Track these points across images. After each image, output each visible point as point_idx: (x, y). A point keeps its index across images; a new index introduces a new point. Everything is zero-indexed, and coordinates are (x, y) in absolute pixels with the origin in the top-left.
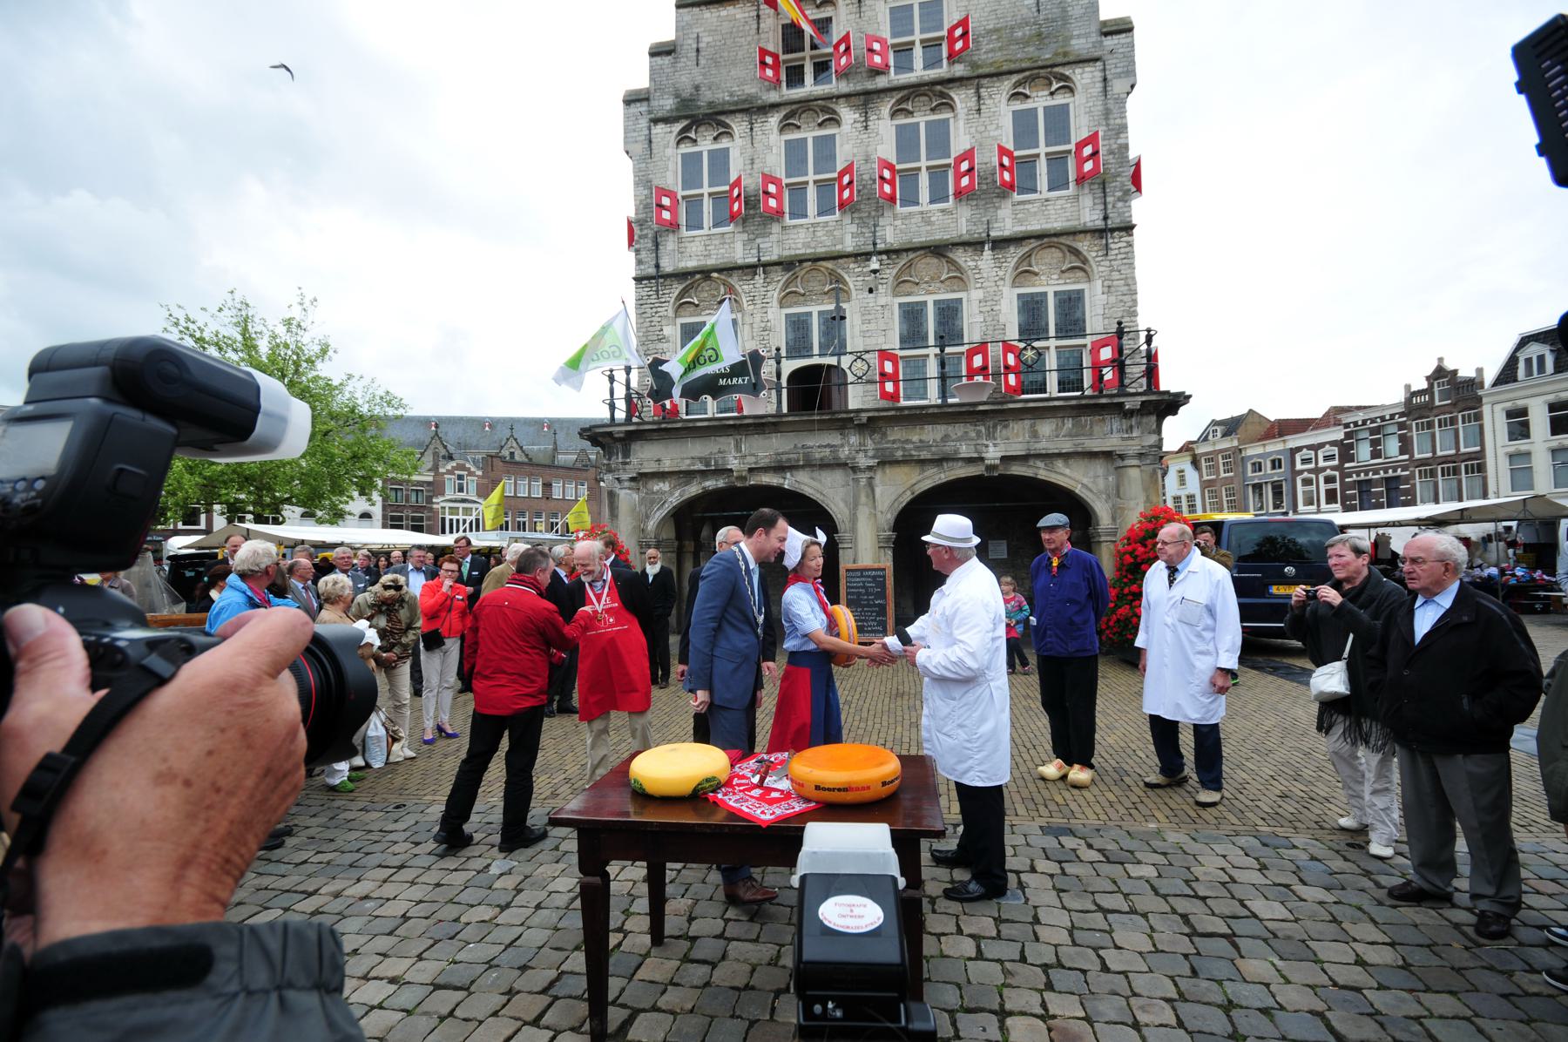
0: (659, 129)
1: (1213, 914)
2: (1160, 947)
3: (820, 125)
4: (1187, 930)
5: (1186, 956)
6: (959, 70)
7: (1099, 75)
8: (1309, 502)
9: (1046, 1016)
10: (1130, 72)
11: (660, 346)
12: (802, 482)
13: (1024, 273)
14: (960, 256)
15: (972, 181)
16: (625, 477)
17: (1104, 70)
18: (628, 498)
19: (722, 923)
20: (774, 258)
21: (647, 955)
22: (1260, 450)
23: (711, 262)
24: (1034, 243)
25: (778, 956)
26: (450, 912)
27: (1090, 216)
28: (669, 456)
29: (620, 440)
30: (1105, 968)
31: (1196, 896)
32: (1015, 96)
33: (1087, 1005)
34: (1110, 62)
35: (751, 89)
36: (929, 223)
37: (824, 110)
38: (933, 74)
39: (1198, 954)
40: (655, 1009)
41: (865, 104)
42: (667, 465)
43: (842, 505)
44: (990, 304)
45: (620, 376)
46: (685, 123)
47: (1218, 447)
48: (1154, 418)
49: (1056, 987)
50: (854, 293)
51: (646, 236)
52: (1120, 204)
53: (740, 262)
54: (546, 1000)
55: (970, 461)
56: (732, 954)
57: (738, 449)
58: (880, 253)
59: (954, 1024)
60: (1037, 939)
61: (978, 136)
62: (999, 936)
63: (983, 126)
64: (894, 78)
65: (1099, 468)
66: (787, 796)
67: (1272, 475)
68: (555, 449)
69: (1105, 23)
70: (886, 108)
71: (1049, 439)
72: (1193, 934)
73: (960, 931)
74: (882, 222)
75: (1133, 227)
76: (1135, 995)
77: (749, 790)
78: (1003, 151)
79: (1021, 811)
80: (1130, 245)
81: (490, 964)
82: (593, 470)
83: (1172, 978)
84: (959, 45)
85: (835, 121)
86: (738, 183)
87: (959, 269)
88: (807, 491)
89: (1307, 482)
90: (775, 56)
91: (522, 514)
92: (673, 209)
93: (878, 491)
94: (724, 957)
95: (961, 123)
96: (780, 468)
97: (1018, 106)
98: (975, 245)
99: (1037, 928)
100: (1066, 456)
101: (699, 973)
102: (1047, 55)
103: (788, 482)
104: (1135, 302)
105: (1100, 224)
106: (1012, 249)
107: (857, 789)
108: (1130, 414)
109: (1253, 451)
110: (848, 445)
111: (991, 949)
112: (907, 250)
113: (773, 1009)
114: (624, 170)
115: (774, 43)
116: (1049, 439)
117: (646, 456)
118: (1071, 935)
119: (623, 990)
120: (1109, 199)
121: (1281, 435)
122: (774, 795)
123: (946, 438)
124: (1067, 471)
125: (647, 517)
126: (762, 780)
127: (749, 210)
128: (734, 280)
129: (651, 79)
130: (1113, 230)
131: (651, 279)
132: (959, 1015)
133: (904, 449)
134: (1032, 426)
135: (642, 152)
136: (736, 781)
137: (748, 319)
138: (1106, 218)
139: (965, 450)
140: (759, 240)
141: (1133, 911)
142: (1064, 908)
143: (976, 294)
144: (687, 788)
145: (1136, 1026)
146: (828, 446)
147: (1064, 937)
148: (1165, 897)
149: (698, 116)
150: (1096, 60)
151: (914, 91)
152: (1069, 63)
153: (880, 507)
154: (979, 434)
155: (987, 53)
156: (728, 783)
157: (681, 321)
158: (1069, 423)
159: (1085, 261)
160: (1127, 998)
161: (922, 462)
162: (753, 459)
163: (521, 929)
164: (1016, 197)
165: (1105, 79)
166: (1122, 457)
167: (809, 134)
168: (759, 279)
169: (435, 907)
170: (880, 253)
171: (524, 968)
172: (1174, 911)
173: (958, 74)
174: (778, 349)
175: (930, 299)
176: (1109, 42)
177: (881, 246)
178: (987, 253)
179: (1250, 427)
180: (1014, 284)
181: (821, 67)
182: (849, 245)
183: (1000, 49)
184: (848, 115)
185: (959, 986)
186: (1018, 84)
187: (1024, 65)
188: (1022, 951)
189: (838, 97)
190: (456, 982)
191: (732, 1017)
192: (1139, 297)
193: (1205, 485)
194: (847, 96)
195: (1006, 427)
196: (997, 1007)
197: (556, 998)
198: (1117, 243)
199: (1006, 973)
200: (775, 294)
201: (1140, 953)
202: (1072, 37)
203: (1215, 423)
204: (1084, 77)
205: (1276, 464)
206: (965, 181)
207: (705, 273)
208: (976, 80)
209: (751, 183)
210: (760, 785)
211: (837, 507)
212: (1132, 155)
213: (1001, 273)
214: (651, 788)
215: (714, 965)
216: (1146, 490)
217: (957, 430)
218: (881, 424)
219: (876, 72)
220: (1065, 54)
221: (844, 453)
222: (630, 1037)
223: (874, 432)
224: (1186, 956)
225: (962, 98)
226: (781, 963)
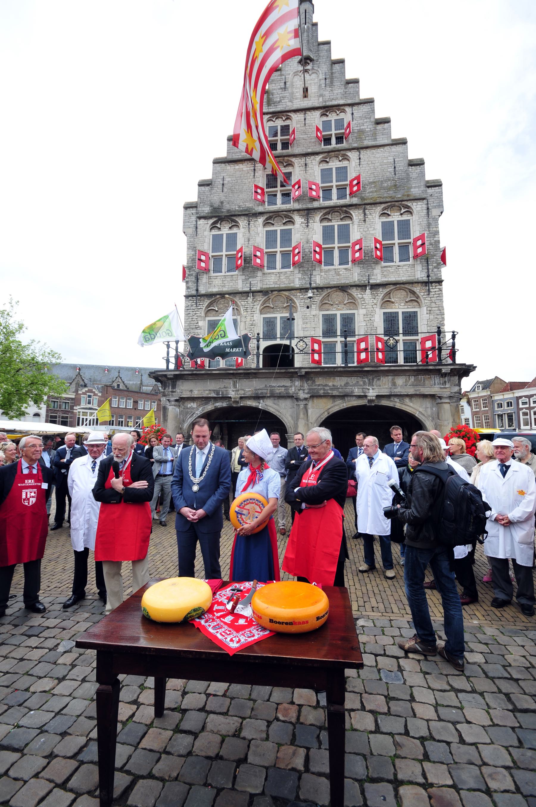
0: (202, 222)
1: (525, 693)
2: (496, 722)
3: (284, 224)
4: (510, 707)
5: (513, 728)
6: (355, 201)
7: (425, 206)
8: (526, 424)
9: (426, 785)
10: (440, 206)
11: (196, 331)
12: (268, 405)
13: (386, 302)
14: (354, 292)
15: (361, 254)
16: (172, 399)
17: (428, 204)
18: (173, 410)
19: (203, 697)
20: (258, 288)
21: (150, 726)
22: (501, 397)
23: (225, 289)
24: (392, 287)
25: (241, 729)
26: (23, 682)
27: (420, 274)
28: (198, 389)
29: (171, 379)
30: (462, 741)
31: (512, 679)
33: (453, 774)
34: (431, 200)
35: (249, 205)
36: (339, 275)
37: (286, 216)
38: (342, 202)
39: (521, 727)
40: (150, 776)
41: (308, 214)
42: (196, 394)
43: (290, 418)
44: (369, 316)
45: (173, 345)
46: (215, 219)
47: (481, 395)
48: (457, 378)
49: (432, 757)
50: (299, 308)
51: (192, 275)
52: (435, 270)
53: (240, 290)
54: (74, 764)
55: (359, 397)
56: (209, 726)
57: (235, 386)
58: (313, 288)
59: (363, 792)
60: (415, 715)
61: (364, 233)
62: (389, 713)
63: (366, 228)
64: (322, 203)
65: (428, 403)
66: (250, 623)
67: (507, 410)
68: (141, 384)
69: (428, 182)
70: (318, 217)
71: (402, 387)
72: (515, 710)
73: (363, 708)
74: (314, 273)
75: (442, 281)
76: (485, 764)
77: (224, 616)
78: (376, 241)
79: (395, 610)
80: (441, 290)
81: (42, 730)
83: (507, 748)
84: (355, 188)
85: (292, 222)
86: (241, 250)
87: (353, 298)
88: (271, 410)
89: (525, 414)
90: (262, 189)
91: (121, 417)
92: (206, 262)
93: (310, 411)
94: (203, 728)
95: (356, 226)
96: (257, 398)
97: (384, 219)
98: (362, 287)
99: (414, 704)
100: (410, 396)
101: (185, 741)
102: (399, 196)
103: (261, 405)
104: (443, 318)
105: (425, 279)
106: (381, 290)
107: (299, 623)
108: (444, 375)
109: (498, 397)
110: (295, 386)
111: (386, 724)
112: (327, 288)
113: (235, 777)
114: (183, 240)
115: (262, 182)
116: (402, 387)
117: (185, 388)
118: (436, 711)
119: (130, 757)
120: (430, 267)
121: (511, 390)
122: (242, 622)
123: (347, 384)
124: (411, 404)
125: (184, 421)
126: (234, 608)
127: (246, 264)
128: (237, 299)
129: (199, 197)
130: (432, 282)
131: (194, 296)
132: (367, 785)
133: (324, 390)
134: (393, 380)
135: (192, 233)
136: (216, 607)
137: (243, 319)
138: (428, 276)
139: (357, 391)
140: (250, 280)
141: (474, 691)
142: (429, 688)
143: (362, 311)
144: (180, 617)
145: (488, 792)
146: (283, 386)
147: (431, 713)
148: (492, 679)
149: (221, 217)
150: (424, 199)
152: (410, 200)
153: (310, 421)
154: (364, 383)
155: (369, 193)
156: (210, 610)
157: (208, 319)
158: (412, 379)
159: (418, 297)
160: (480, 767)
161: (334, 397)
162: (243, 392)
163: (68, 699)
164: (383, 264)
165: (428, 209)
166: (440, 398)
167: (278, 228)
168: (250, 299)
169: (16, 677)
170: (313, 288)
171: (64, 734)
172: (500, 691)
173: (354, 203)
174: (258, 334)
175: (338, 313)
176: (430, 191)
177: (314, 285)
178: (368, 291)
179: (496, 385)
180: (381, 307)
181: (286, 195)
182: (297, 284)
183: (376, 191)
184: (298, 219)
185: (364, 756)
186: (384, 209)
187: (387, 200)
188: (406, 726)
189: (294, 211)
190: (16, 744)
191: (206, 785)
192: (446, 316)
193: (474, 414)
194: (298, 210)
195: (379, 379)
196: (391, 777)
197: (82, 763)
198: (434, 289)
199: (396, 744)
200: (258, 307)
201: (483, 727)
202: (411, 188)
203: (478, 382)
205: (509, 404)
206: (357, 255)
207: (222, 295)
208: (364, 206)
209: (248, 250)
210: (232, 612)
211: (287, 419)
212: (442, 246)
213: (375, 301)
214: (154, 615)
215: (195, 735)
216: (453, 416)
217: (353, 380)
218: (312, 375)
219: (313, 199)
220: (408, 196)
221: (292, 390)
222: (129, 802)
223: (308, 380)
224: (513, 728)
225: (356, 214)
226: (243, 734)
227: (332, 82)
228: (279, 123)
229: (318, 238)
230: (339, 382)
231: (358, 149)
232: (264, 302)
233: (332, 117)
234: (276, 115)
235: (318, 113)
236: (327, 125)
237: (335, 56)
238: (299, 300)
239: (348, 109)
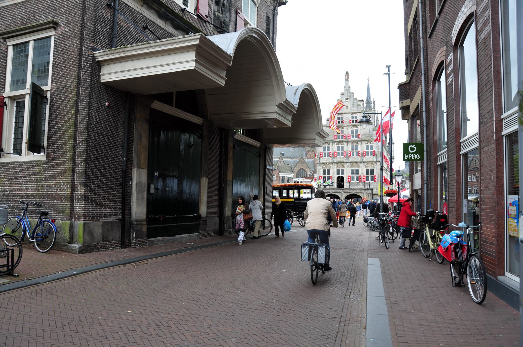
6: (359, 139)
13: (366, 166)
14: (359, 163)
27: (375, 160)
35: (333, 139)
37: (342, 142)
44: (362, 170)
64: (352, 139)
70: (350, 143)
82: (277, 171)
151: (353, 141)
155: (363, 138)
182: (345, 161)
208: (361, 141)
209: (333, 152)
211: (340, 196)
225: (360, 143)
228: (340, 116)
229: (350, 149)
230: (348, 190)
233: (354, 115)
234: (339, 114)
236: (352, 117)
237: (355, 97)
238: (345, 165)
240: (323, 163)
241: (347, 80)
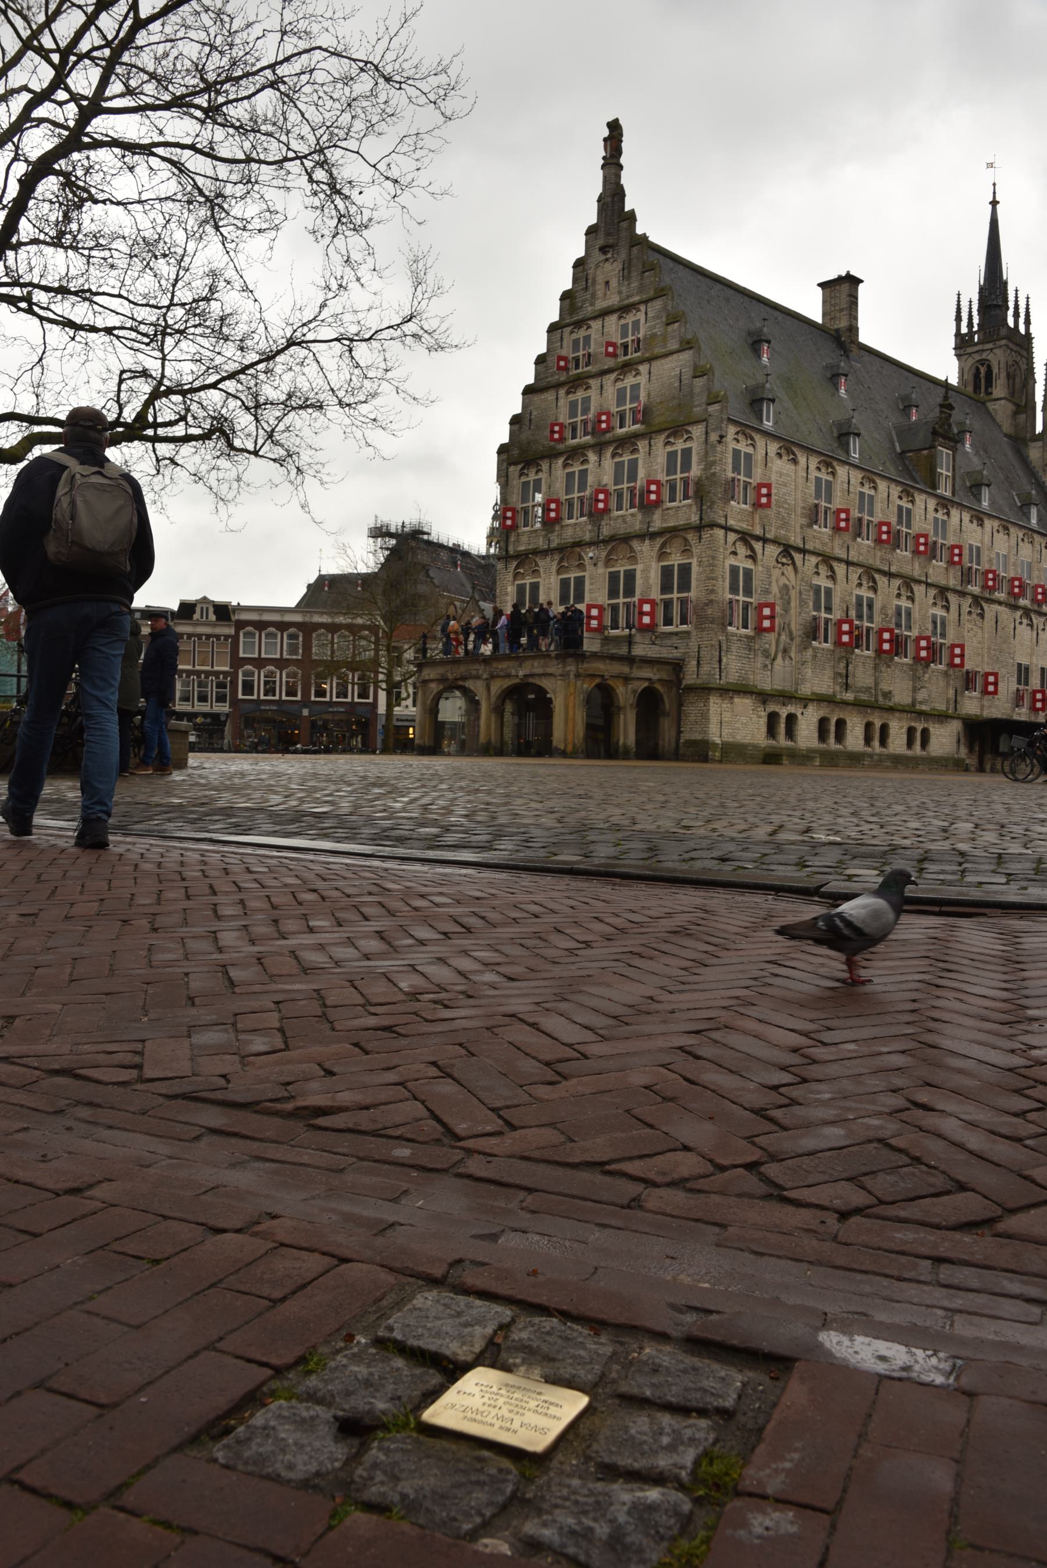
0: (512, 468)
13: (662, 555)
14: (636, 544)
24: (668, 535)
27: (695, 519)
32: (667, 443)
36: (625, 522)
42: (432, 676)
44: (646, 570)
70: (610, 451)
74: (603, 523)
85: (586, 461)
138: (701, 519)
168: (548, 558)
176: (711, 409)
182: (587, 537)
184: (592, 457)
200: (554, 568)
204: (697, 431)
225: (642, 445)
227: (629, 272)
228: (582, 333)
231: (650, 360)
232: (561, 560)
233: (630, 319)
234: (578, 324)
235: (614, 317)
239: (642, 308)
240: (517, 556)
241: (612, 162)
